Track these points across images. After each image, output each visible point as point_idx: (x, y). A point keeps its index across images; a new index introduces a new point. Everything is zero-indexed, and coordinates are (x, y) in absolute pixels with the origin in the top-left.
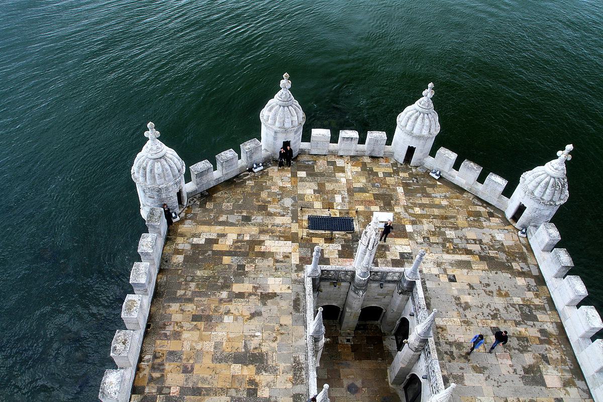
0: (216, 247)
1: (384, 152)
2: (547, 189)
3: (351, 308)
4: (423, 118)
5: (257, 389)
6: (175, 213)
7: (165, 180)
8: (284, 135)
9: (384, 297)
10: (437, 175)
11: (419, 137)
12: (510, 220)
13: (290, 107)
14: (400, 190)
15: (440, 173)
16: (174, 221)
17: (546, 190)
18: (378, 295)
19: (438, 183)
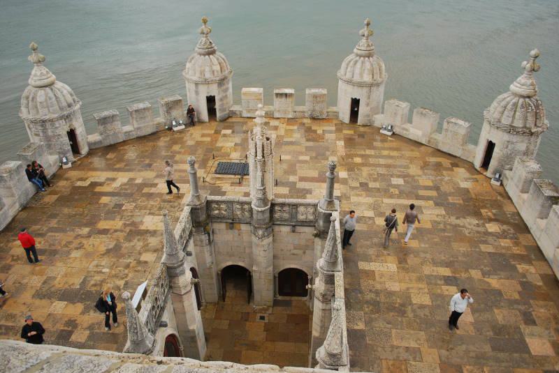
0: (98, 189)
1: (327, 112)
2: (515, 111)
3: (258, 265)
4: (363, 62)
5: (73, 332)
6: (67, 159)
7: (49, 110)
8: (206, 86)
9: (304, 253)
10: (389, 131)
11: (361, 85)
12: (479, 169)
13: (211, 56)
14: (341, 143)
15: (392, 127)
16: (64, 167)
17: (515, 114)
18: (295, 248)
19: (389, 138)
